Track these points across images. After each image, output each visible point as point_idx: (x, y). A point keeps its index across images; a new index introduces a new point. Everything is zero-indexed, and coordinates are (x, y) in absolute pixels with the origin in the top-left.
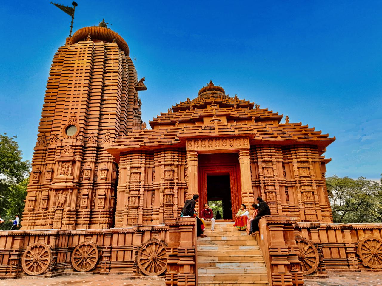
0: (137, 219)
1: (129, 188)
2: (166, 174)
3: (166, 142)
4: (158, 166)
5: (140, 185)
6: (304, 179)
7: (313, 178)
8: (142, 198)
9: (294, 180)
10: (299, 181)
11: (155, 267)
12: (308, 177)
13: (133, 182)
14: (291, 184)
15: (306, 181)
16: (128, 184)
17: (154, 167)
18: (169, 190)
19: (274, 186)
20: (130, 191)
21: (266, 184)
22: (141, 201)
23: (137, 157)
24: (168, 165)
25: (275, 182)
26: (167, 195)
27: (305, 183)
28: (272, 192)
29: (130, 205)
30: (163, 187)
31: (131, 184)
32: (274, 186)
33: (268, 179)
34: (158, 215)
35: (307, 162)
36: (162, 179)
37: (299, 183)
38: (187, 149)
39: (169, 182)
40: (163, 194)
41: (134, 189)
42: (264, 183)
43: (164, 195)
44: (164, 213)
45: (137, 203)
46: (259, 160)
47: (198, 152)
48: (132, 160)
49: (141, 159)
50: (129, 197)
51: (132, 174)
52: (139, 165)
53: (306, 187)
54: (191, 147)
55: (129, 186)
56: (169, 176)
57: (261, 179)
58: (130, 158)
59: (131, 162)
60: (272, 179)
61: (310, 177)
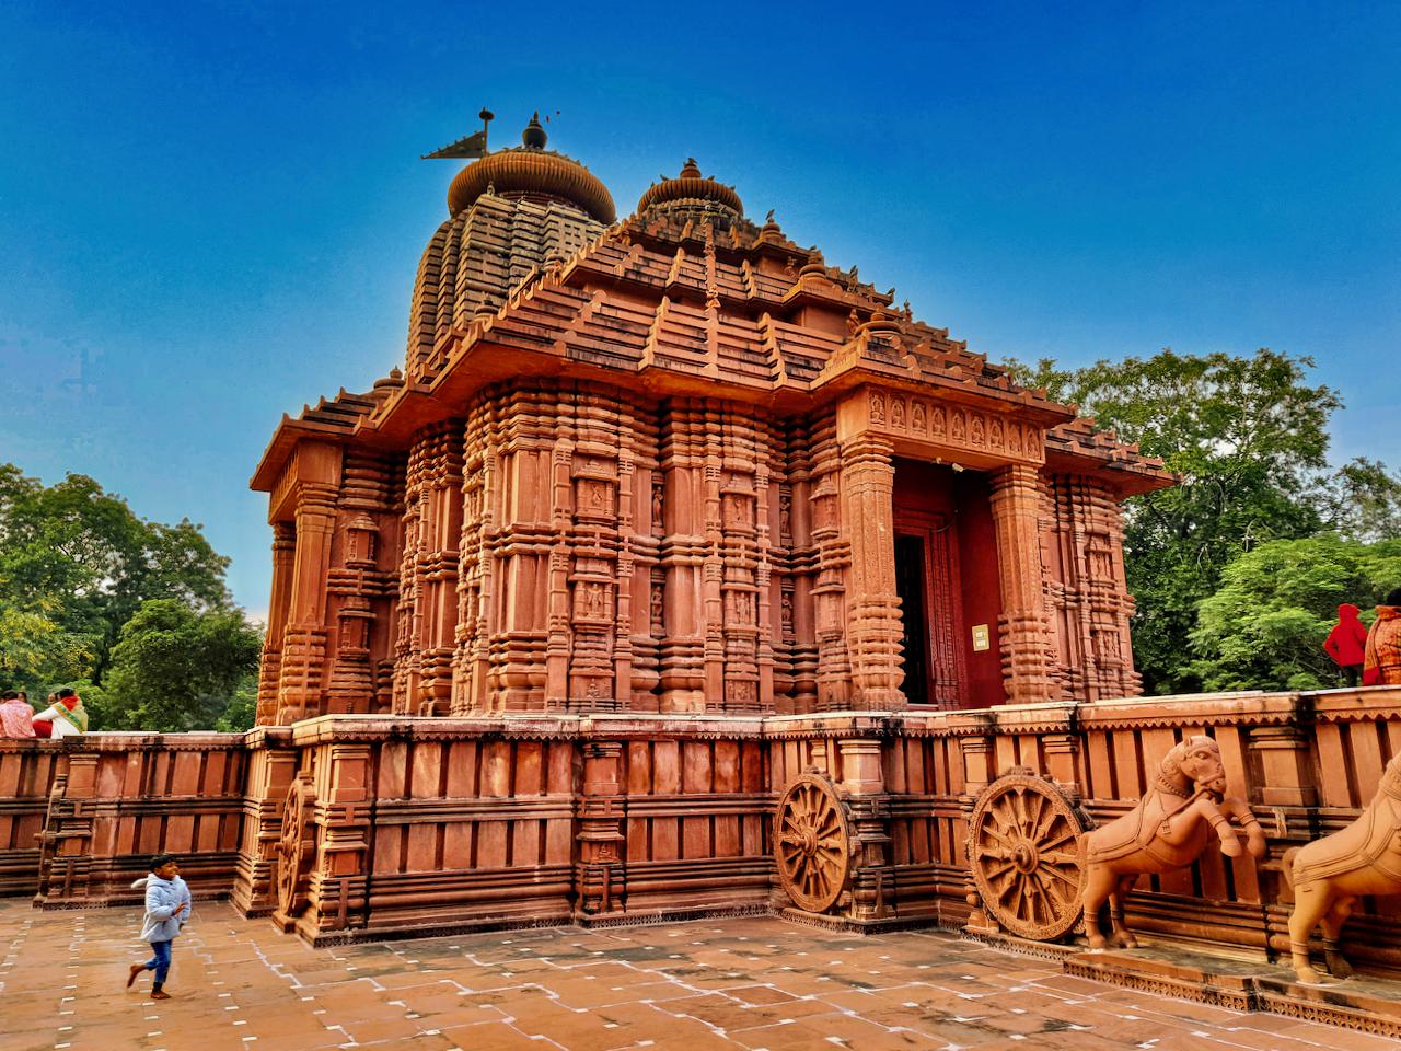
0: (609, 681)
1: (573, 544)
3: (597, 352)
5: (618, 539)
6: (590, 528)
7: (625, 531)
8: (624, 594)
9: (702, 541)
10: (568, 534)
11: (1037, 897)
13: (587, 520)
14: (690, 555)
15: (597, 539)
16: (568, 525)
18: (741, 574)
19: (754, 571)
20: (573, 558)
21: (728, 559)
22: (624, 603)
25: (759, 554)
26: (737, 592)
27: (593, 544)
29: (578, 618)
30: (569, 550)
31: (580, 528)
32: (754, 571)
34: (703, 673)
36: (563, 514)
37: (568, 543)
39: (743, 541)
40: (715, 587)
41: (597, 550)
43: (723, 593)
44: (725, 664)
45: (608, 610)
47: (899, 443)
49: (618, 423)
50: (571, 585)
51: (728, 500)
52: (614, 450)
55: (574, 534)
56: (739, 519)
60: (751, 543)
61: (615, 526)
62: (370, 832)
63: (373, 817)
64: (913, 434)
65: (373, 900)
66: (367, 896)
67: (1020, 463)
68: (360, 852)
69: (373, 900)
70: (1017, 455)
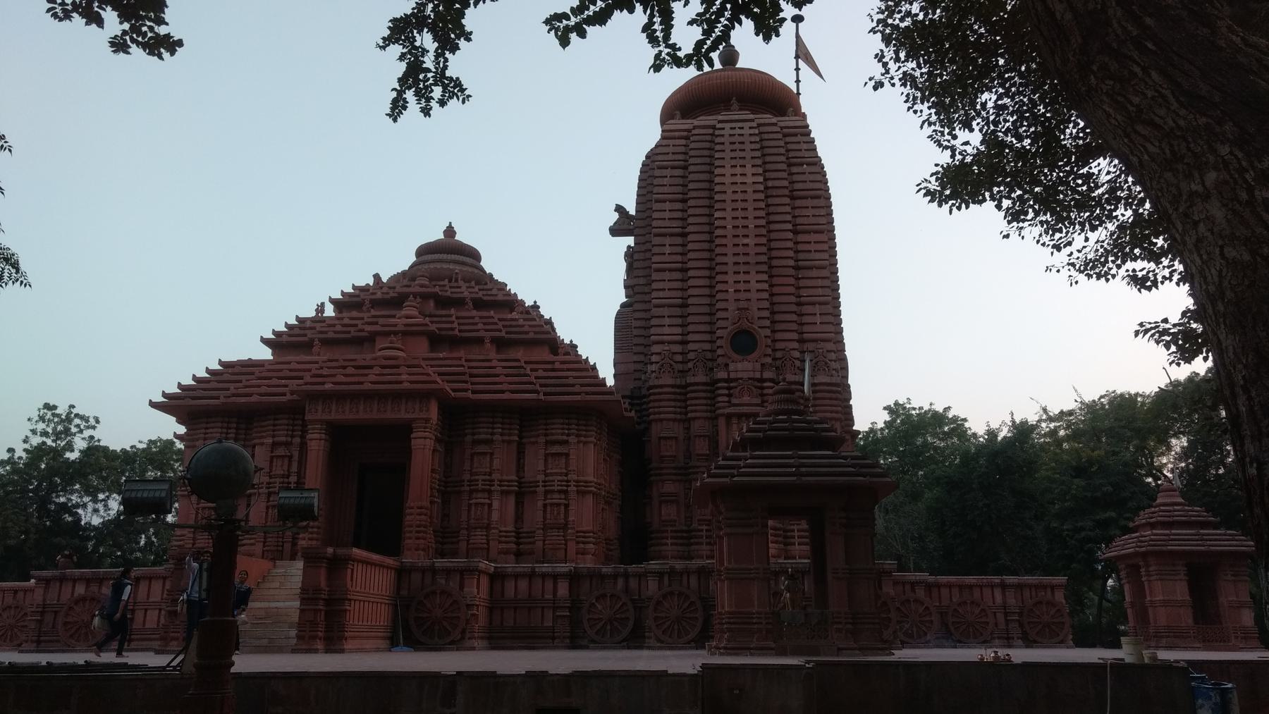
2: (274, 464)
4: (262, 444)
12: (561, 474)
17: (254, 447)
23: (220, 425)
24: (280, 444)
28: (483, 504)
33: (477, 477)
34: (253, 547)
35: (566, 442)
38: (308, 417)
40: (265, 504)
42: (469, 486)
43: (267, 508)
46: (469, 438)
48: (208, 431)
53: (556, 496)
54: (316, 413)
57: (467, 477)
58: (204, 425)
59: (205, 434)
62: (42, 613)
63: (44, 608)
64: (334, 416)
65: (42, 638)
66: (39, 636)
67: (414, 420)
68: (37, 620)
69: (42, 638)
70: (413, 416)
